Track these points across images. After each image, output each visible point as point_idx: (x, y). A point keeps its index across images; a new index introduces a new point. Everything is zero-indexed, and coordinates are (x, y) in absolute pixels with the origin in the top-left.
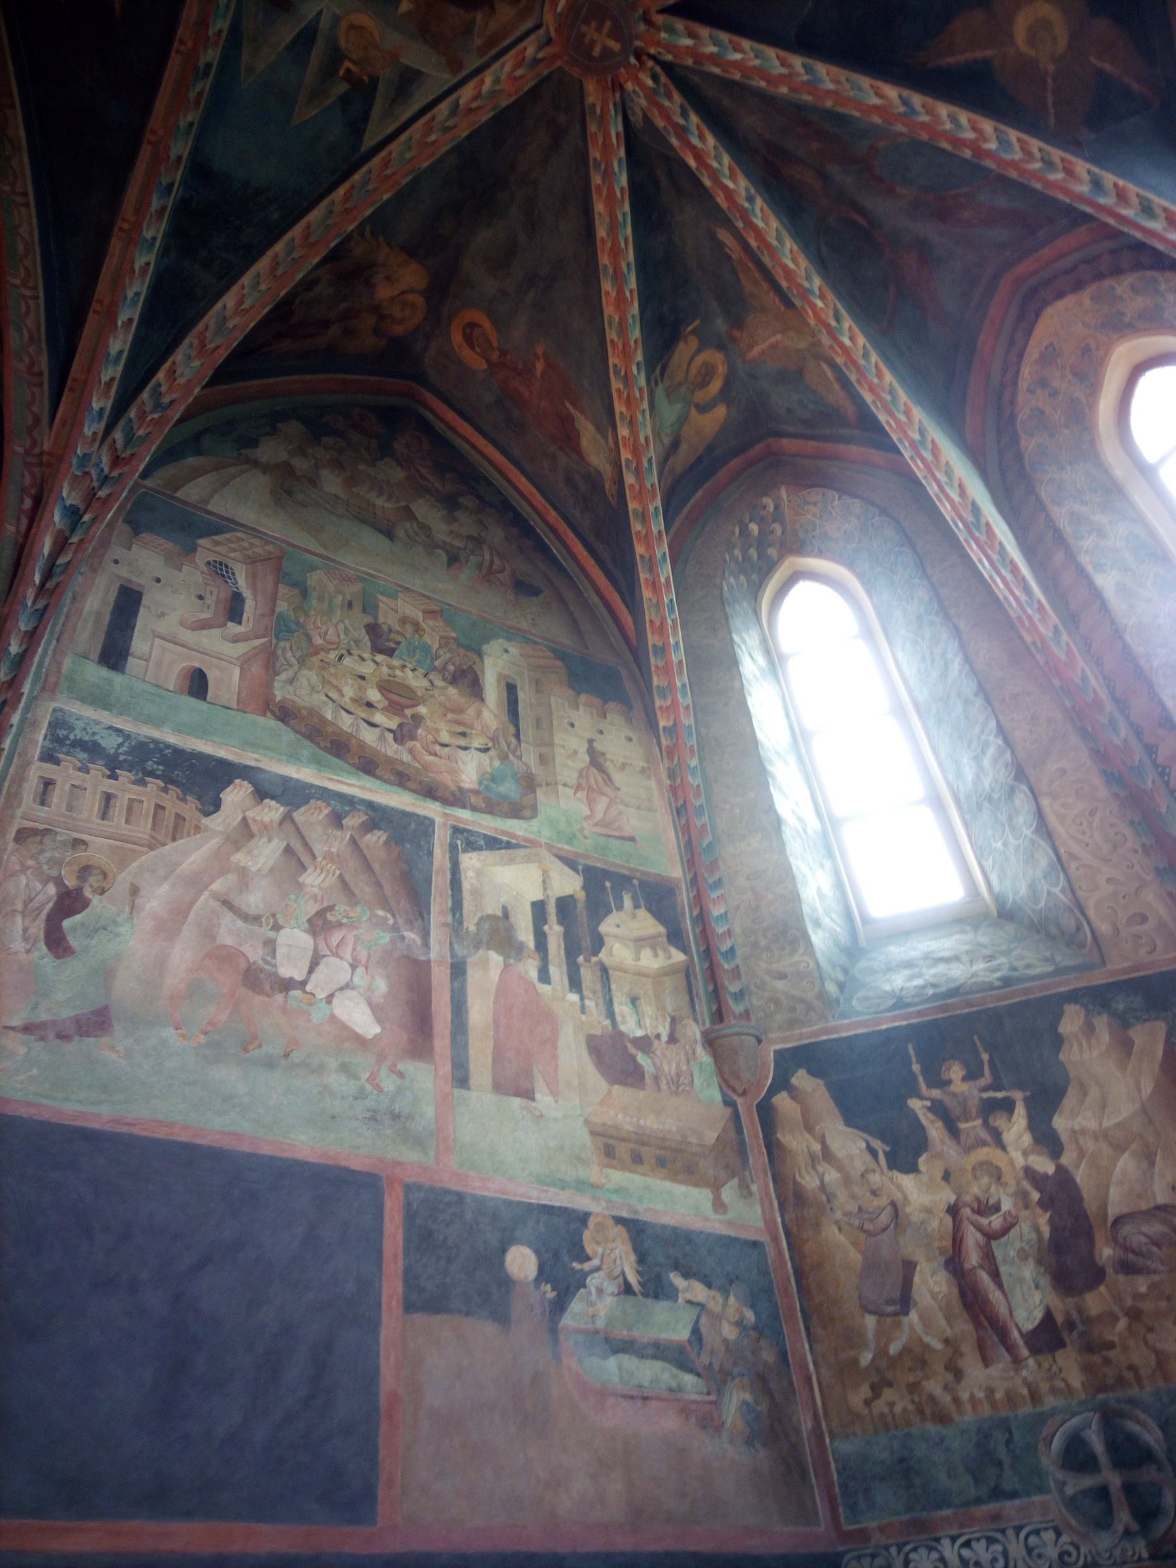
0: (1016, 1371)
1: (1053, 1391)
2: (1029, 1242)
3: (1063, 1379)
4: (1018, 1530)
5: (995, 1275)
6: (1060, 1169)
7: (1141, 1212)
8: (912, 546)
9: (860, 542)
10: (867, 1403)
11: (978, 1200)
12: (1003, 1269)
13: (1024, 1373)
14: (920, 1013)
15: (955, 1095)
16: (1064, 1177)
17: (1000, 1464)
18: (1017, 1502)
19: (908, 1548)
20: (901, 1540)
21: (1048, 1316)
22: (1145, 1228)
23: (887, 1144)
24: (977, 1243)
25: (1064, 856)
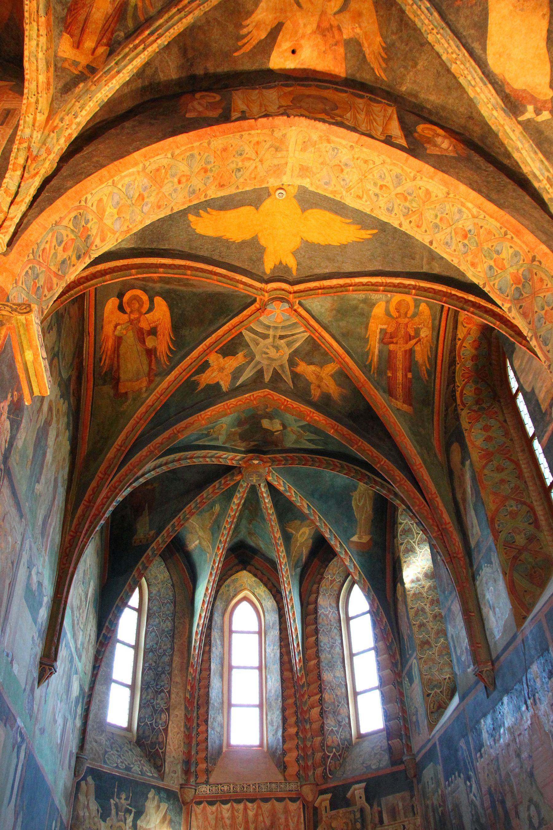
8: (175, 607)
14: (122, 773)
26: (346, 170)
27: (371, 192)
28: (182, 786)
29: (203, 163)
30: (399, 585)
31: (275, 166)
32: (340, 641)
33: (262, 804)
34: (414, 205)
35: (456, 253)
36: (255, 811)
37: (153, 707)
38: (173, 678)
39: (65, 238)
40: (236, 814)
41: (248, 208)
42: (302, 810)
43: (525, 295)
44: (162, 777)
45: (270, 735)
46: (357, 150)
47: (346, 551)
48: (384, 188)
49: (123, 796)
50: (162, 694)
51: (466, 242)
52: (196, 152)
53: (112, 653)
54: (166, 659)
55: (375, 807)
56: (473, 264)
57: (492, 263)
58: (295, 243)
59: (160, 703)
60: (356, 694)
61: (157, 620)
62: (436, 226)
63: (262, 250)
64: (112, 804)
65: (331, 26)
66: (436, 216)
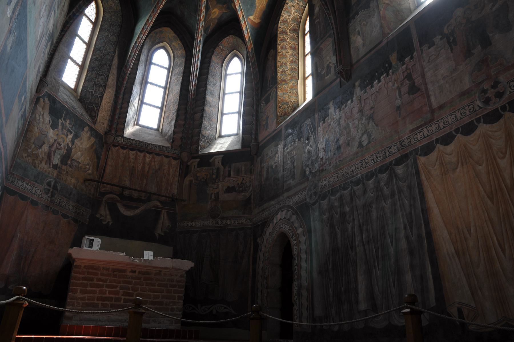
0: (49, 168)
1: (52, 174)
2: (61, 153)
3: (54, 174)
4: (36, 188)
5: (54, 154)
6: (72, 147)
7: (76, 161)
9: (111, 12)
10: (26, 157)
11: (59, 142)
12: (56, 154)
13: (50, 169)
15: (66, 124)
16: (71, 149)
17: (39, 178)
18: (38, 184)
19: (19, 180)
20: (18, 178)
21: (57, 164)
22: (75, 163)
23: (53, 123)
24: (55, 147)
25: (101, 105)
28: (106, 133)
30: (272, 51)
32: (219, 84)
33: (155, 156)
36: (150, 159)
37: (95, 82)
38: (112, 69)
40: (138, 157)
42: (179, 165)
44: (95, 123)
45: (165, 124)
47: (245, 22)
49: (68, 121)
50: (103, 76)
53: (80, 21)
54: (109, 57)
55: (227, 169)
59: (100, 80)
60: (223, 114)
61: (106, 33)
64: (60, 123)
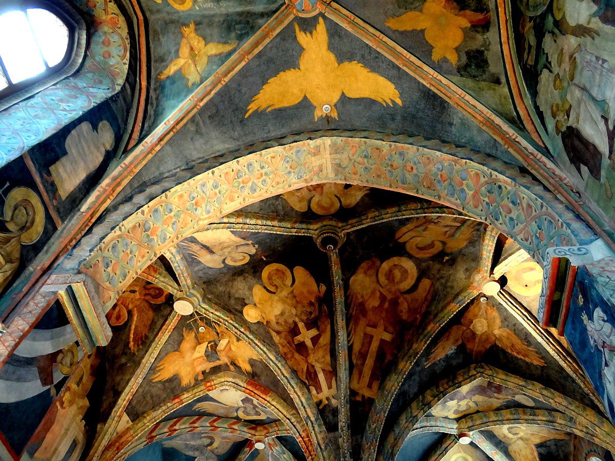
26: (289, 169)
27: (267, 166)
29: (394, 173)
31: (339, 153)
34: (236, 184)
35: (195, 188)
39: (508, 218)
41: (351, 96)
43: (144, 234)
46: (287, 186)
48: (259, 176)
51: (193, 202)
52: (400, 184)
56: (181, 196)
57: (172, 214)
58: (304, 62)
62: (216, 187)
63: (331, 47)
65: (314, 190)
66: (220, 193)
